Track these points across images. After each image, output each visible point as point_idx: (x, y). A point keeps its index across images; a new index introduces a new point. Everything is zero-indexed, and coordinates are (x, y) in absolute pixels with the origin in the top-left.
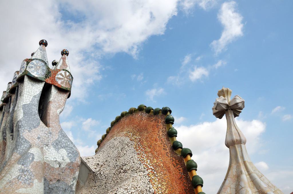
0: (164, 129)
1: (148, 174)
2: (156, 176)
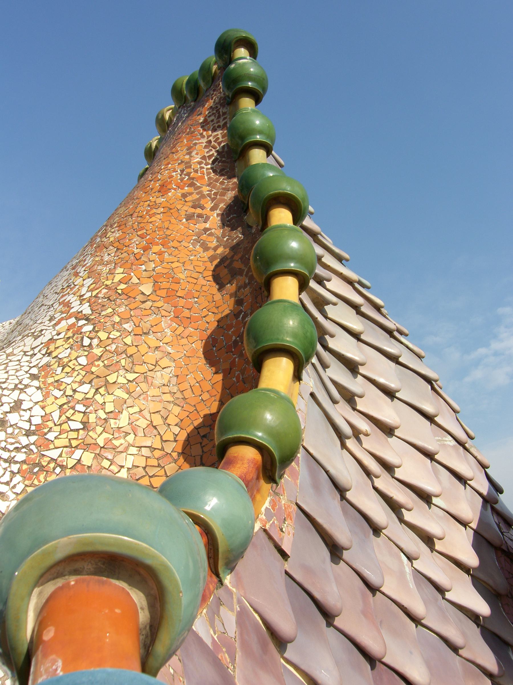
1: (51, 339)
2: (86, 342)
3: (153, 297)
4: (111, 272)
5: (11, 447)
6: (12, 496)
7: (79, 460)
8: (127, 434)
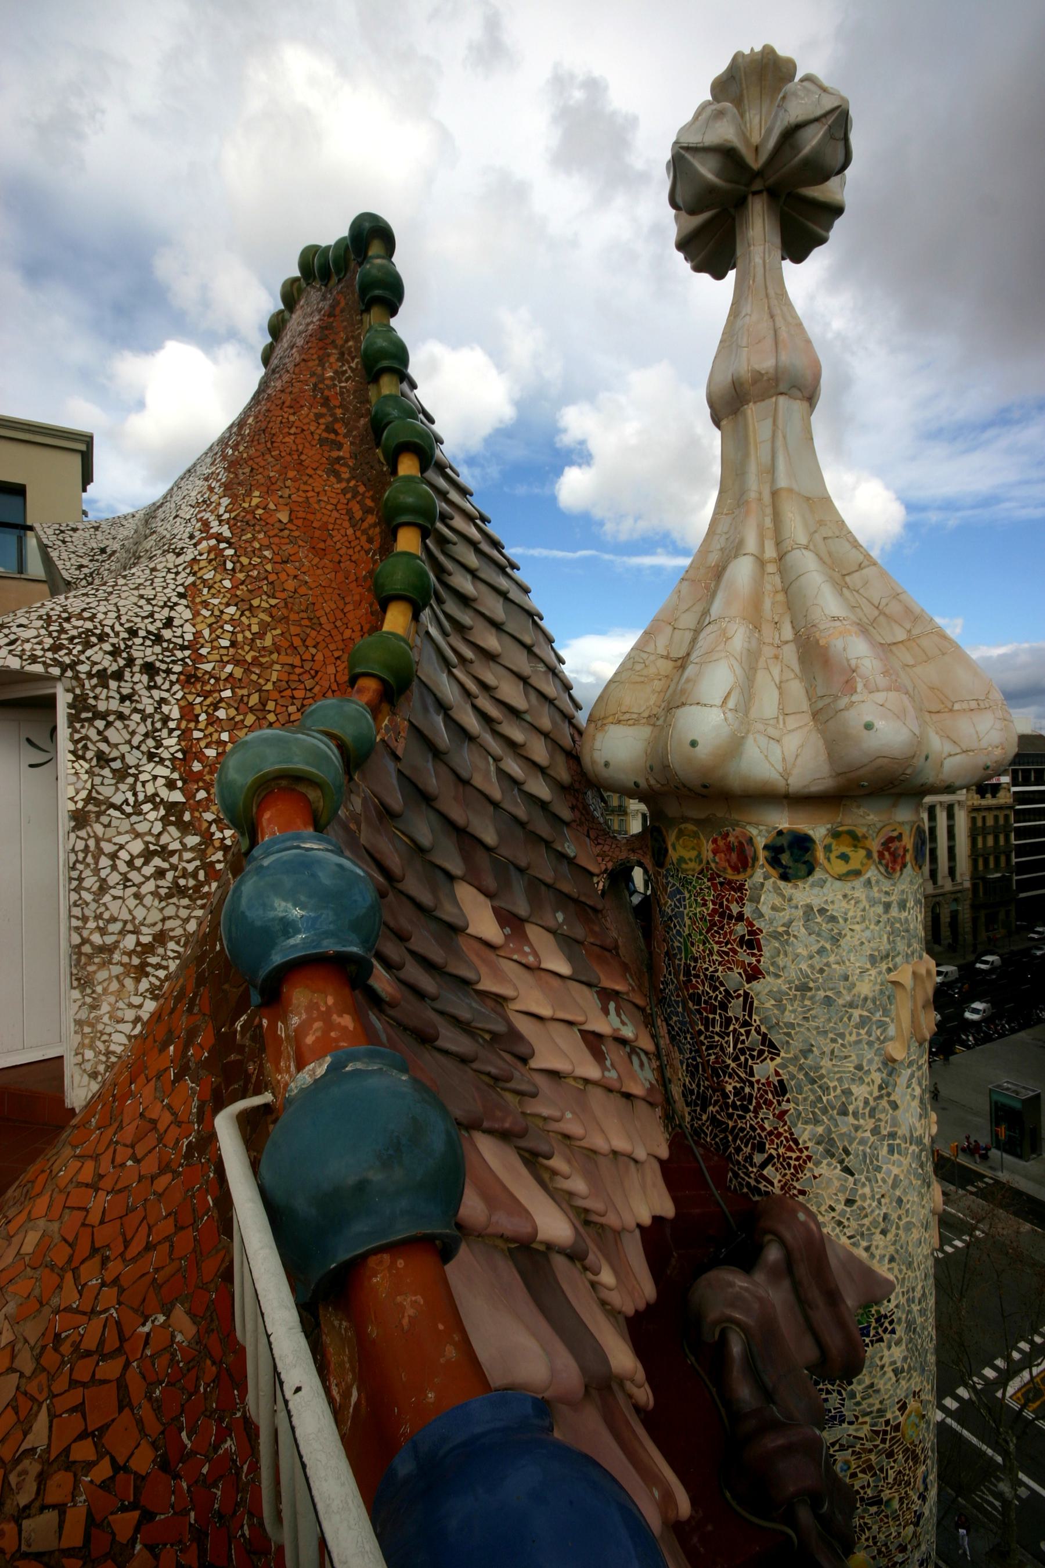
0: (351, 343)
2: (229, 565)
3: (289, 526)
4: (249, 494)
5: (168, 660)
6: (174, 702)
7: (231, 674)
8: (272, 653)
